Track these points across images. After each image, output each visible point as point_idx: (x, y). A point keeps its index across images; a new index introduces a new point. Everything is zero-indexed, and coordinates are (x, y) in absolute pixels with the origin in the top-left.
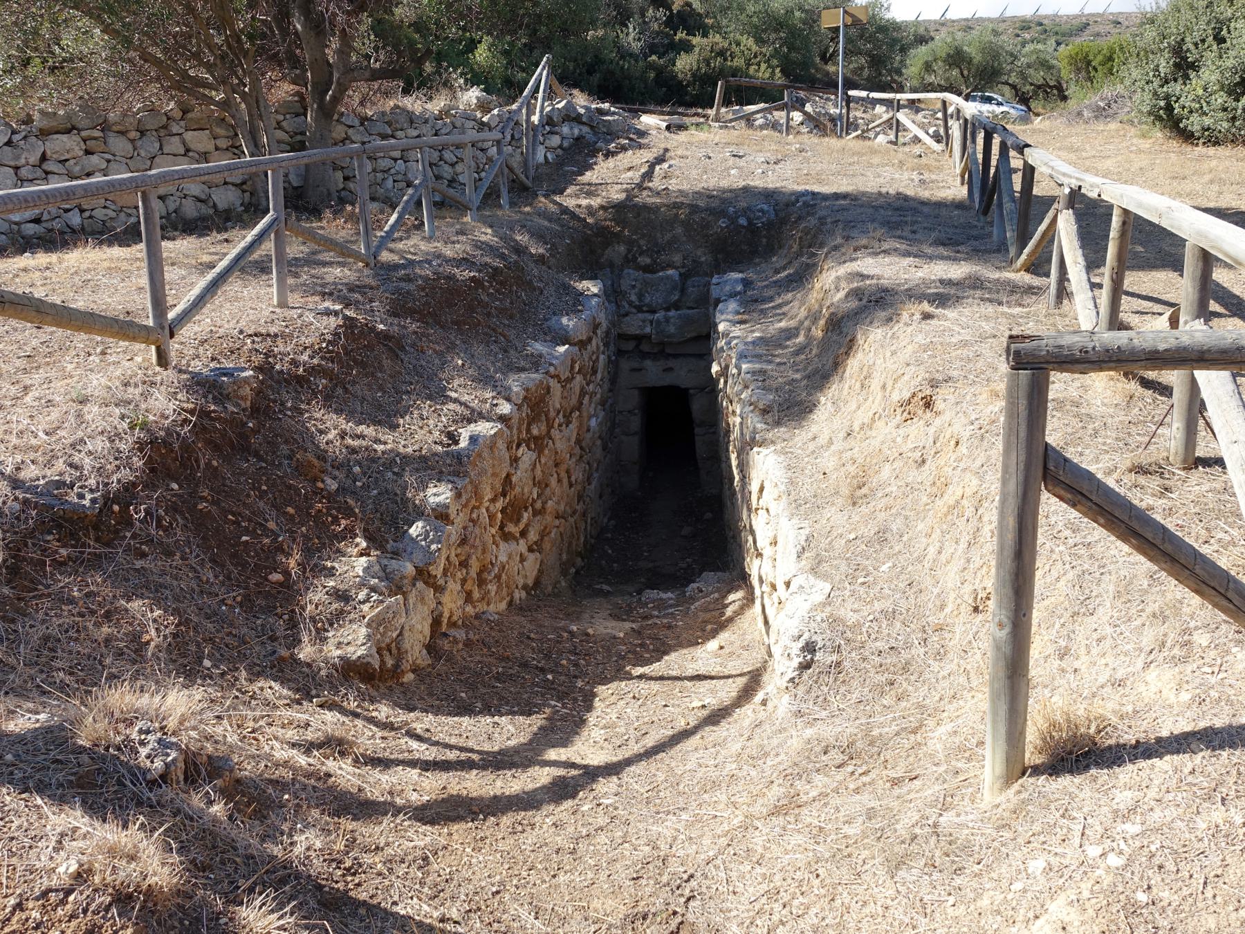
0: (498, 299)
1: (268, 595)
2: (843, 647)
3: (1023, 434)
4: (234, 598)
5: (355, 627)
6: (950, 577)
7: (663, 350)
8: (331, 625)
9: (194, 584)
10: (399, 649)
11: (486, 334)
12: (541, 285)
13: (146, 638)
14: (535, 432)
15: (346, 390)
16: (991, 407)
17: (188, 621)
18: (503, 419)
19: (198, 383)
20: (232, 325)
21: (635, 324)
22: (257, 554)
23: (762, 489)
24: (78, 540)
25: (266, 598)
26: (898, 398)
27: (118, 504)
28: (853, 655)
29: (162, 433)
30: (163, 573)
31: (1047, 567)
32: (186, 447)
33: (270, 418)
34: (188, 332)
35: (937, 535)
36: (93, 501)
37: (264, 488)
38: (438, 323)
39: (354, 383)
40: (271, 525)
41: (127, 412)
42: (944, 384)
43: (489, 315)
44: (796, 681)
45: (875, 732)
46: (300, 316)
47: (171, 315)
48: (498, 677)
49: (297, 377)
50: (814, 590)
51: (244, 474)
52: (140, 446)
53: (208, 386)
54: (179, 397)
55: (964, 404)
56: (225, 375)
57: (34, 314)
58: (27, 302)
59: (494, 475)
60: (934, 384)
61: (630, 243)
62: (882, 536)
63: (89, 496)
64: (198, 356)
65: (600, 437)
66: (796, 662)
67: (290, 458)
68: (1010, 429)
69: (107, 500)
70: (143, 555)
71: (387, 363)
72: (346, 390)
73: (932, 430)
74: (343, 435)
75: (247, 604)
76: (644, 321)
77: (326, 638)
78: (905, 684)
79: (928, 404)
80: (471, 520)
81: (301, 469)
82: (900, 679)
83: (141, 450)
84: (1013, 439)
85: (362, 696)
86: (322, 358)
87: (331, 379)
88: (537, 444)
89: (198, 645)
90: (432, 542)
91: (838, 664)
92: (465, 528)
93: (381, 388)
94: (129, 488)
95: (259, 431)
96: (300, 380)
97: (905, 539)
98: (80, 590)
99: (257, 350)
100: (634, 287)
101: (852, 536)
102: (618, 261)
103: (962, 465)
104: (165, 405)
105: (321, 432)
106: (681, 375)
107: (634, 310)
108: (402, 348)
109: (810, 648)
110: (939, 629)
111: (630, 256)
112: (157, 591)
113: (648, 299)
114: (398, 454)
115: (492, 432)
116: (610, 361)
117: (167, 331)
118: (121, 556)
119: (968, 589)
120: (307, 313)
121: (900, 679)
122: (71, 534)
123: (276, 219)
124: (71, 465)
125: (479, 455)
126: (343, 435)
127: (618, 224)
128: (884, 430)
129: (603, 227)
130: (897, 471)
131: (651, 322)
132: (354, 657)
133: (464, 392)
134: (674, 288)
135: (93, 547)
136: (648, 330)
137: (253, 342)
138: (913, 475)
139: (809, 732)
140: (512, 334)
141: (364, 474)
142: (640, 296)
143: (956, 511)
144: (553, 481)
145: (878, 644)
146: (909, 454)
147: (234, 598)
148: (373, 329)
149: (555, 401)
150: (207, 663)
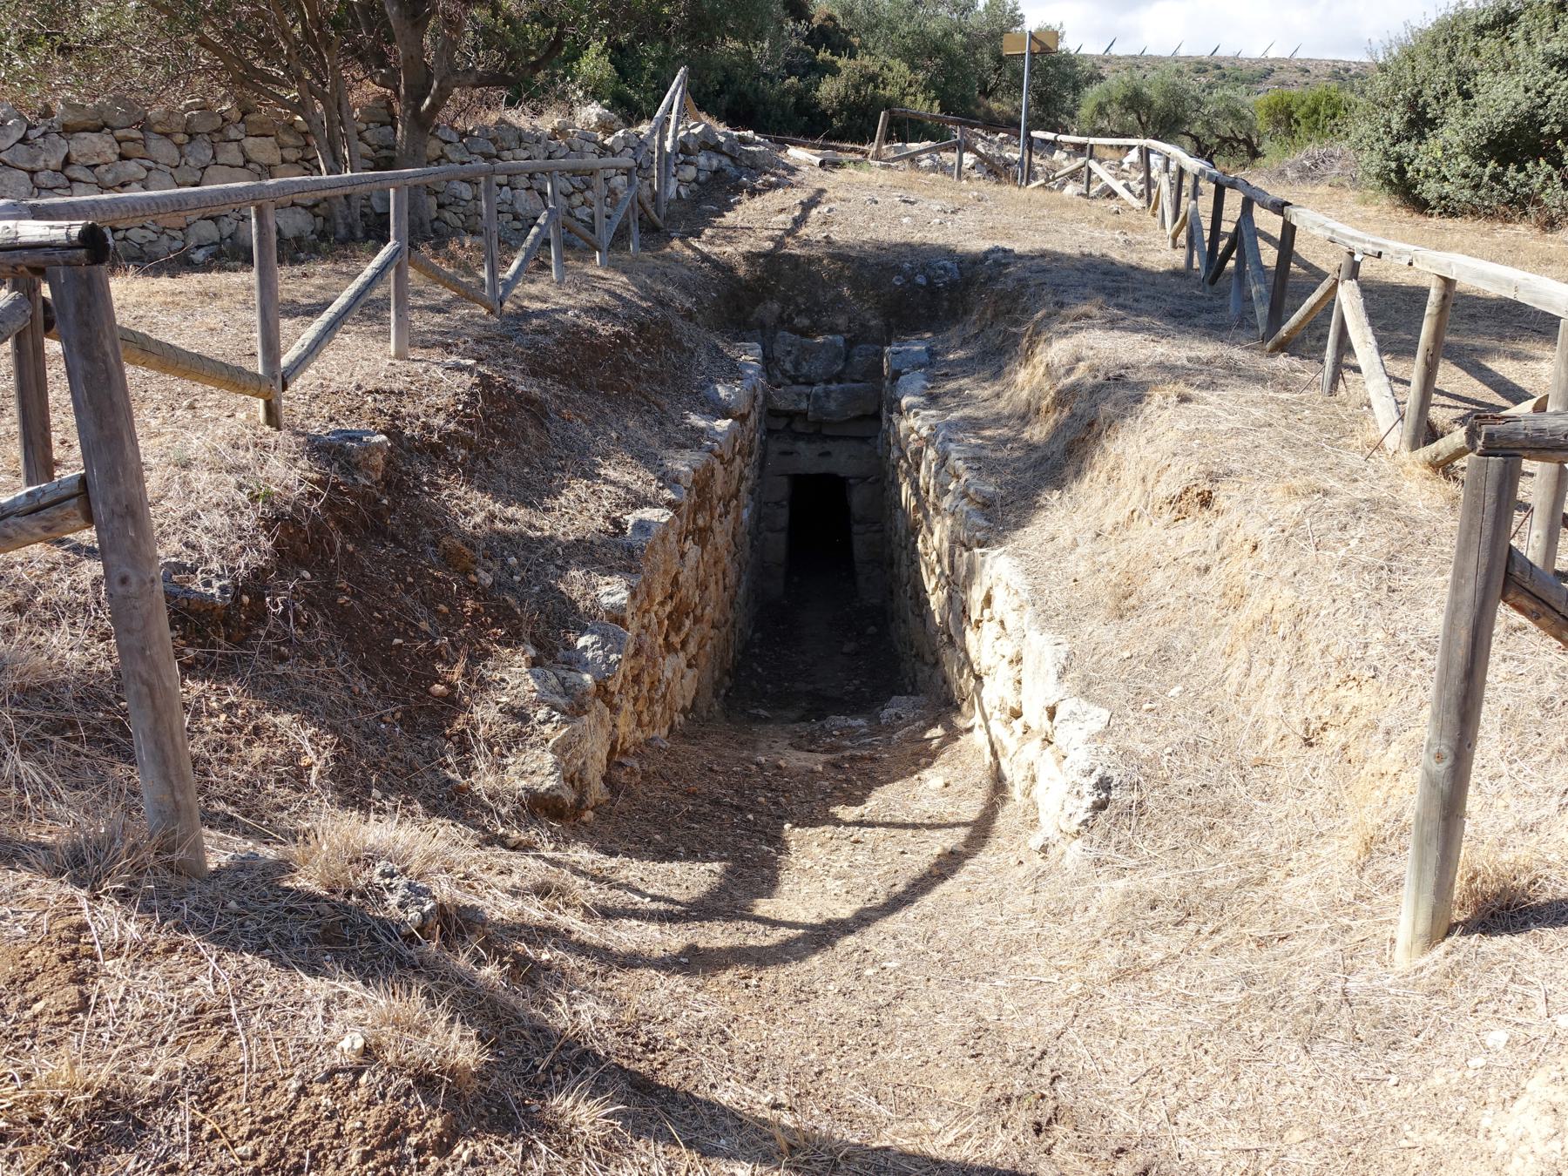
0: (647, 361)
1: (431, 712)
2: (1143, 783)
3: (1487, 532)
4: (393, 714)
5: (538, 752)
6: (1269, 706)
7: (819, 430)
8: (509, 749)
9: (345, 696)
10: (581, 780)
11: (637, 402)
12: (691, 345)
13: (305, 761)
14: (700, 522)
15: (489, 465)
16: (1290, 508)
17: (348, 741)
18: (670, 504)
19: (318, 449)
20: (344, 377)
21: (786, 399)
22: (413, 662)
23: (988, 601)
24: (206, 638)
25: (429, 715)
26: (1165, 494)
27: (248, 594)
28: (1156, 793)
29: (289, 508)
30: (309, 682)
31: (1403, 694)
32: (317, 527)
33: (405, 495)
34: (295, 386)
35: (1242, 655)
36: (223, 589)
37: (410, 579)
38: (581, 386)
39: (498, 455)
40: (424, 625)
41: (241, 480)
42: (1225, 479)
43: (638, 379)
44: (1090, 823)
45: (1208, 884)
46: (426, 371)
47: (285, 361)
48: (691, 817)
49: (432, 445)
50: (1088, 717)
51: (384, 562)
52: (268, 525)
53: (329, 451)
54: (300, 463)
55: (1255, 503)
56: (351, 439)
57: (138, 352)
58: (131, 337)
59: (666, 572)
60: (1213, 478)
62: (1164, 655)
63: (216, 584)
64: (312, 415)
66: (1088, 801)
67: (435, 544)
68: (1471, 526)
69: (238, 590)
70: (283, 659)
71: (531, 431)
72: (489, 465)
73: (1213, 532)
74: (492, 517)
75: (408, 721)
76: (799, 395)
77: (505, 767)
78: (1229, 829)
79: (1206, 501)
80: (643, 627)
81: (449, 559)
82: (1220, 822)
83: (267, 528)
84: (1475, 537)
85: (554, 837)
86: (460, 423)
87: (471, 450)
88: (701, 536)
89: (363, 771)
90: (611, 651)
91: (1140, 804)
92: (638, 636)
93: (528, 463)
94: (258, 574)
95: (394, 511)
96: (436, 450)
97: (1194, 658)
98: (218, 701)
99: (381, 411)
100: (789, 353)
101: (1126, 654)
103: (1265, 573)
104: (287, 474)
105: (466, 514)
106: (842, 460)
108: (546, 415)
109: (1104, 784)
110: (1261, 764)
112: (304, 704)
113: (805, 368)
114: (559, 544)
115: (664, 520)
116: (761, 442)
117: (279, 382)
118: (258, 659)
119: (1296, 718)
120: (434, 367)
121: (1220, 822)
122: (198, 631)
123: (398, 250)
124: (187, 545)
125: (652, 548)
126: (492, 517)
128: (1147, 534)
130: (1173, 579)
131: (808, 396)
132: (542, 789)
133: (621, 473)
135: (223, 647)
136: (804, 405)
137: (375, 400)
138: (1194, 584)
139: (1120, 884)
140: (665, 401)
141: (522, 566)
142: (797, 365)
143: (1265, 627)
144: (712, 587)
145: (1185, 781)
146: (1187, 560)
147: (393, 714)
148: (512, 390)
149: (718, 488)
150: (376, 793)
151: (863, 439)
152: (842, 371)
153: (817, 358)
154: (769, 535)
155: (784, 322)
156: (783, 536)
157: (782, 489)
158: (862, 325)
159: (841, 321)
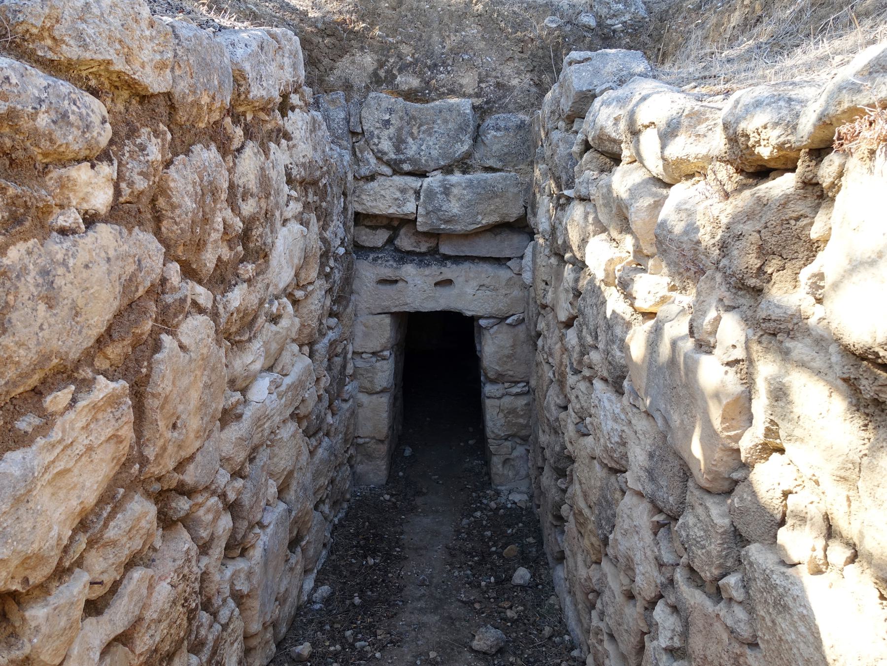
7: (436, 246)
21: (387, 196)
61: (384, 49)
65: (295, 416)
76: (403, 191)
100: (387, 123)
102: (359, 80)
106: (469, 292)
111: (382, 73)
113: (412, 149)
127: (362, 18)
129: (335, 22)
131: (417, 193)
134: (462, 129)
136: (410, 207)
142: (399, 143)
151: (500, 261)
152: (469, 155)
154: (364, 398)
155: (380, 80)
156: (384, 401)
158: (498, 85)
159: (468, 80)
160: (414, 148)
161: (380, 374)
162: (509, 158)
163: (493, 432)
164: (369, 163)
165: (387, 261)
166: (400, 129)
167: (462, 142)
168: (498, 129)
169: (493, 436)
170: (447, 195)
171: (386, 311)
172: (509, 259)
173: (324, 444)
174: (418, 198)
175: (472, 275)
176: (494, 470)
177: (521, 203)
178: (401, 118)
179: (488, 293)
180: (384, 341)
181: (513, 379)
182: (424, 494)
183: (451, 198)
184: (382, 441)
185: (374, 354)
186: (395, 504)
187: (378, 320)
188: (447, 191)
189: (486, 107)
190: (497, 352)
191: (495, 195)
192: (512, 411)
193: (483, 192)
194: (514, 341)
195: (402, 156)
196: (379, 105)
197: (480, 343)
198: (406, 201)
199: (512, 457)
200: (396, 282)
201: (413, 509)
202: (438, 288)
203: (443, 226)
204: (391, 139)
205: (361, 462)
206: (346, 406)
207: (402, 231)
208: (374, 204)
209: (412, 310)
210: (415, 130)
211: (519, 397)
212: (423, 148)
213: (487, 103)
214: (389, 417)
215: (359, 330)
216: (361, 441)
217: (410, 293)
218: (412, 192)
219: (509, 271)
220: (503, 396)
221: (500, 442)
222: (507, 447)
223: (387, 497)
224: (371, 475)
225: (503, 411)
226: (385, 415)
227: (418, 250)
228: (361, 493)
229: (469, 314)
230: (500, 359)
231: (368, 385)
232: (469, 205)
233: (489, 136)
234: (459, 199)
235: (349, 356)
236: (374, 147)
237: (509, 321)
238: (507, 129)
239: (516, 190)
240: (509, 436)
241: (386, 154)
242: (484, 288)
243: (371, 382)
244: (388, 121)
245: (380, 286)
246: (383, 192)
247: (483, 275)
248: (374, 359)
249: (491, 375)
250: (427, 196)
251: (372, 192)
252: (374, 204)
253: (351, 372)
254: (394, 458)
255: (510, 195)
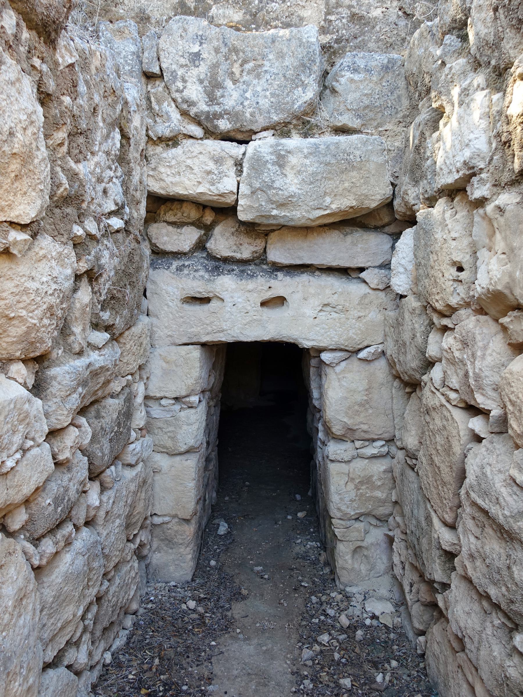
76: (218, 161)
100: (196, 58)
106: (307, 314)
107: (197, 131)
113: (231, 97)
131: (239, 164)
134: (303, 67)
136: (228, 184)
142: (213, 88)
152: (312, 109)
153: (257, 72)
154: (162, 461)
156: (190, 466)
157: (182, 373)
160: (235, 95)
161: (185, 427)
162: (371, 115)
163: (339, 509)
164: (169, 119)
165: (196, 271)
166: (215, 66)
167: (304, 86)
168: (356, 70)
169: (339, 515)
170: (281, 166)
171: (194, 340)
172: (362, 270)
173: (78, 545)
174: (240, 172)
175: (312, 290)
176: (340, 563)
177: (388, 178)
178: (217, 50)
179: (334, 315)
180: (190, 382)
181: (367, 436)
182: (244, 598)
183: (287, 170)
184: (187, 521)
185: (176, 399)
186: (202, 616)
187: (183, 353)
188: (281, 160)
189: (336, 46)
190: (346, 398)
191: (351, 166)
192: (367, 481)
193: (333, 161)
194: (370, 382)
195: (217, 108)
196: (185, 30)
197: (320, 387)
198: (222, 175)
199: (364, 544)
200: (206, 300)
201: (227, 626)
202: (265, 309)
203: (275, 212)
204: (201, 82)
205: (158, 550)
206: (129, 474)
207: (218, 230)
208: (177, 179)
209: (230, 340)
210: (236, 69)
211: (374, 461)
212: (248, 95)
213: (337, 41)
214: (197, 487)
215: (156, 367)
216: (157, 520)
217: (227, 316)
218: (230, 162)
219: (363, 285)
220: (353, 458)
221: (349, 523)
222: (359, 531)
223: (192, 604)
224: (172, 568)
225: (353, 479)
226: (192, 484)
227: (238, 256)
228: (156, 596)
229: (306, 344)
230: (349, 408)
231: (169, 443)
232: (314, 180)
233: (343, 80)
234: (299, 172)
235: (139, 399)
236: (177, 95)
237: (361, 355)
238: (368, 70)
239: (381, 159)
240: (362, 515)
241: (191, 104)
242: (328, 309)
243: (173, 438)
244: (197, 55)
245: (186, 306)
246: (189, 162)
247: (328, 291)
248: (177, 407)
249: (337, 429)
250: (252, 167)
251: (173, 162)
252: (177, 179)
253: (142, 424)
254: (205, 537)
255: (372, 166)
